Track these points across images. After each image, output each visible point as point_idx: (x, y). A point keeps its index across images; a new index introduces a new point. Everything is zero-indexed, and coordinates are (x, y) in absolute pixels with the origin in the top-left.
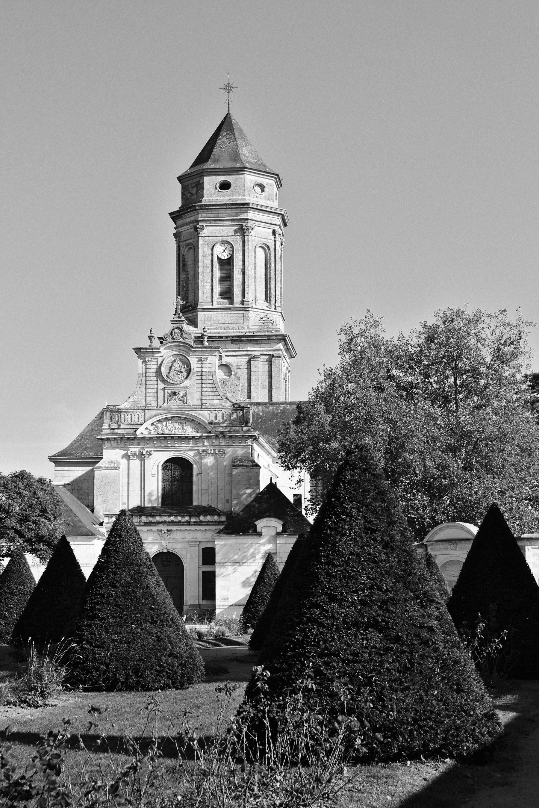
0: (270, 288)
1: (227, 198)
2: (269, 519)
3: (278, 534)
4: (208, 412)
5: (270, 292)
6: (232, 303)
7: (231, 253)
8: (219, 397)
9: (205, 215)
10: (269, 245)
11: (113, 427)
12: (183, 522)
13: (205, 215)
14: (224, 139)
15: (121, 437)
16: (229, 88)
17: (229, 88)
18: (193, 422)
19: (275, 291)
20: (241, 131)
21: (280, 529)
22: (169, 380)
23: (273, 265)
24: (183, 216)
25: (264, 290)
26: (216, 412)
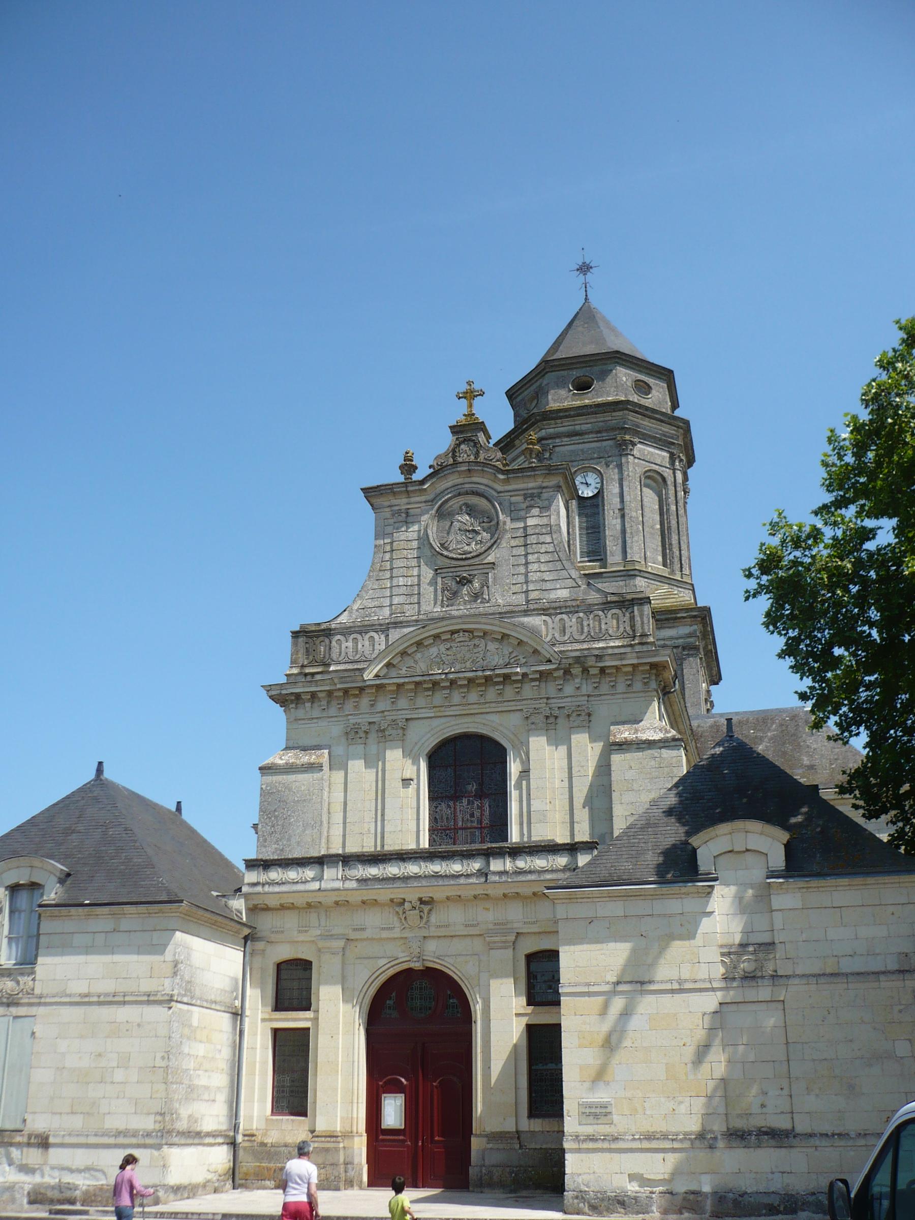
0: (671, 544)
1: (587, 401)
2: (739, 824)
3: (772, 874)
4: (544, 617)
5: (671, 550)
6: (603, 562)
7: (599, 486)
8: (570, 583)
9: (552, 431)
10: (665, 475)
11: (307, 670)
12: (468, 876)
13: (552, 431)
14: (580, 329)
15: (327, 688)
16: (585, 269)
17: (585, 269)
18: (505, 642)
19: (680, 550)
20: (608, 324)
21: (778, 860)
22: (445, 553)
23: (673, 508)
24: (517, 442)
25: (660, 548)
26: (564, 616)
